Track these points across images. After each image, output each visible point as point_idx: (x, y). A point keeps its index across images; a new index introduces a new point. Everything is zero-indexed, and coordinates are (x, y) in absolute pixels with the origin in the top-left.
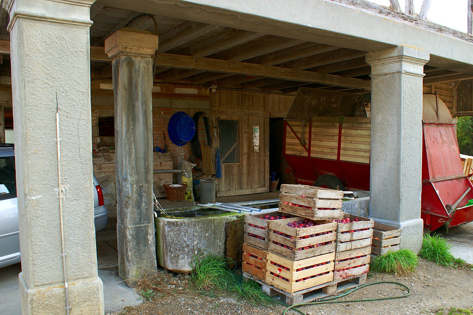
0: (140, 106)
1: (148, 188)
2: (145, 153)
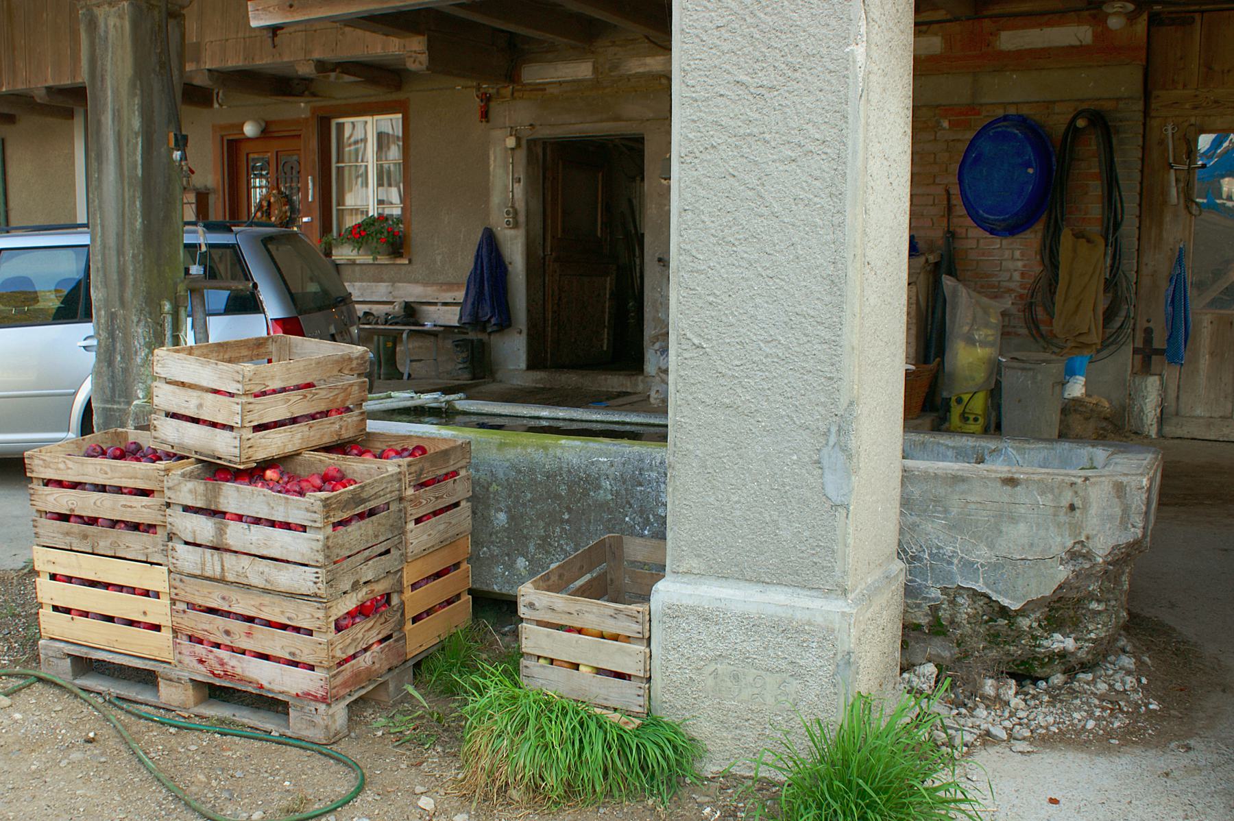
0: (110, 122)
1: (125, 319)
2: (117, 234)
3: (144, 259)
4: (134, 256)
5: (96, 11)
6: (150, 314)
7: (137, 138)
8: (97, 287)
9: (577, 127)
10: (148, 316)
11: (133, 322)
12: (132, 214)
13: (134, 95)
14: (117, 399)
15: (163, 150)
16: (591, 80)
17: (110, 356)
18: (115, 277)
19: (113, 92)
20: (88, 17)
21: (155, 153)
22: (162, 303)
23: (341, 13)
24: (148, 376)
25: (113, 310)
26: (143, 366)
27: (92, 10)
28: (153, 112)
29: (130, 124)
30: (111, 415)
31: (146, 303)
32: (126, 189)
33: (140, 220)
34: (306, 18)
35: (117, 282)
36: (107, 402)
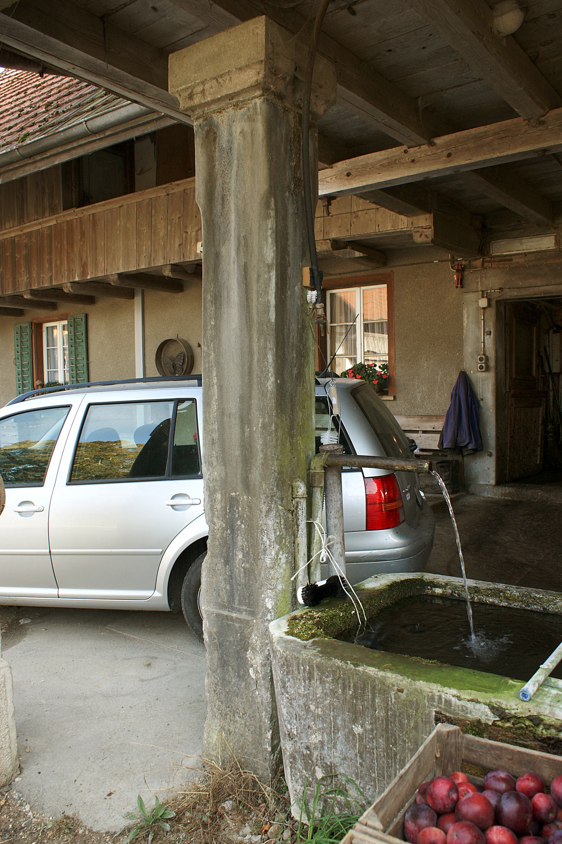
0: (233, 253)
1: (250, 507)
2: (242, 397)
3: (276, 431)
4: (264, 427)
5: (217, 118)
6: (282, 500)
7: (269, 272)
8: (210, 464)
9: (542, 289)
10: (279, 503)
11: (261, 512)
12: (262, 372)
13: (268, 216)
14: (236, 605)
15: (296, 288)
16: (552, 250)
17: (228, 552)
18: (237, 452)
19: (238, 216)
20: (206, 128)
21: (289, 293)
22: (294, 484)
23: (400, 176)
24: (278, 579)
25: (234, 494)
26: (272, 568)
27: (211, 117)
28: (287, 240)
29: (261, 255)
30: (229, 625)
31: (277, 486)
32: (255, 339)
33: (272, 379)
34: (364, 184)
35: (239, 460)
36: (223, 607)
